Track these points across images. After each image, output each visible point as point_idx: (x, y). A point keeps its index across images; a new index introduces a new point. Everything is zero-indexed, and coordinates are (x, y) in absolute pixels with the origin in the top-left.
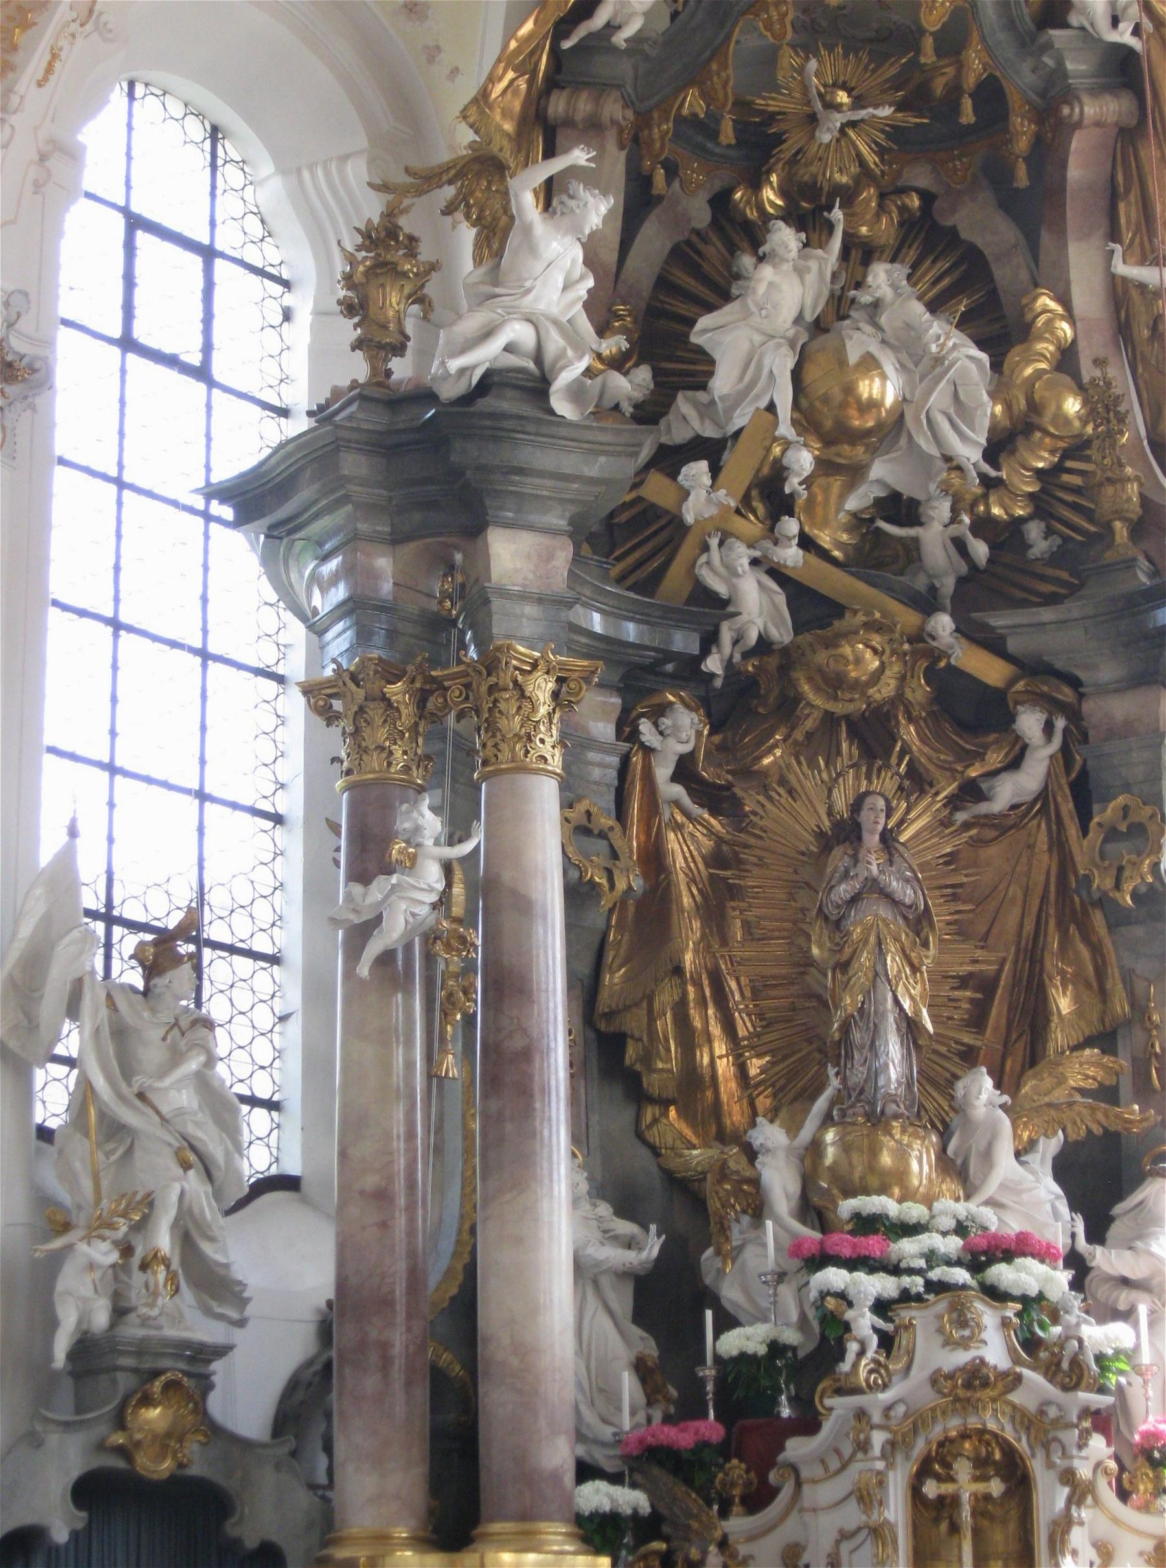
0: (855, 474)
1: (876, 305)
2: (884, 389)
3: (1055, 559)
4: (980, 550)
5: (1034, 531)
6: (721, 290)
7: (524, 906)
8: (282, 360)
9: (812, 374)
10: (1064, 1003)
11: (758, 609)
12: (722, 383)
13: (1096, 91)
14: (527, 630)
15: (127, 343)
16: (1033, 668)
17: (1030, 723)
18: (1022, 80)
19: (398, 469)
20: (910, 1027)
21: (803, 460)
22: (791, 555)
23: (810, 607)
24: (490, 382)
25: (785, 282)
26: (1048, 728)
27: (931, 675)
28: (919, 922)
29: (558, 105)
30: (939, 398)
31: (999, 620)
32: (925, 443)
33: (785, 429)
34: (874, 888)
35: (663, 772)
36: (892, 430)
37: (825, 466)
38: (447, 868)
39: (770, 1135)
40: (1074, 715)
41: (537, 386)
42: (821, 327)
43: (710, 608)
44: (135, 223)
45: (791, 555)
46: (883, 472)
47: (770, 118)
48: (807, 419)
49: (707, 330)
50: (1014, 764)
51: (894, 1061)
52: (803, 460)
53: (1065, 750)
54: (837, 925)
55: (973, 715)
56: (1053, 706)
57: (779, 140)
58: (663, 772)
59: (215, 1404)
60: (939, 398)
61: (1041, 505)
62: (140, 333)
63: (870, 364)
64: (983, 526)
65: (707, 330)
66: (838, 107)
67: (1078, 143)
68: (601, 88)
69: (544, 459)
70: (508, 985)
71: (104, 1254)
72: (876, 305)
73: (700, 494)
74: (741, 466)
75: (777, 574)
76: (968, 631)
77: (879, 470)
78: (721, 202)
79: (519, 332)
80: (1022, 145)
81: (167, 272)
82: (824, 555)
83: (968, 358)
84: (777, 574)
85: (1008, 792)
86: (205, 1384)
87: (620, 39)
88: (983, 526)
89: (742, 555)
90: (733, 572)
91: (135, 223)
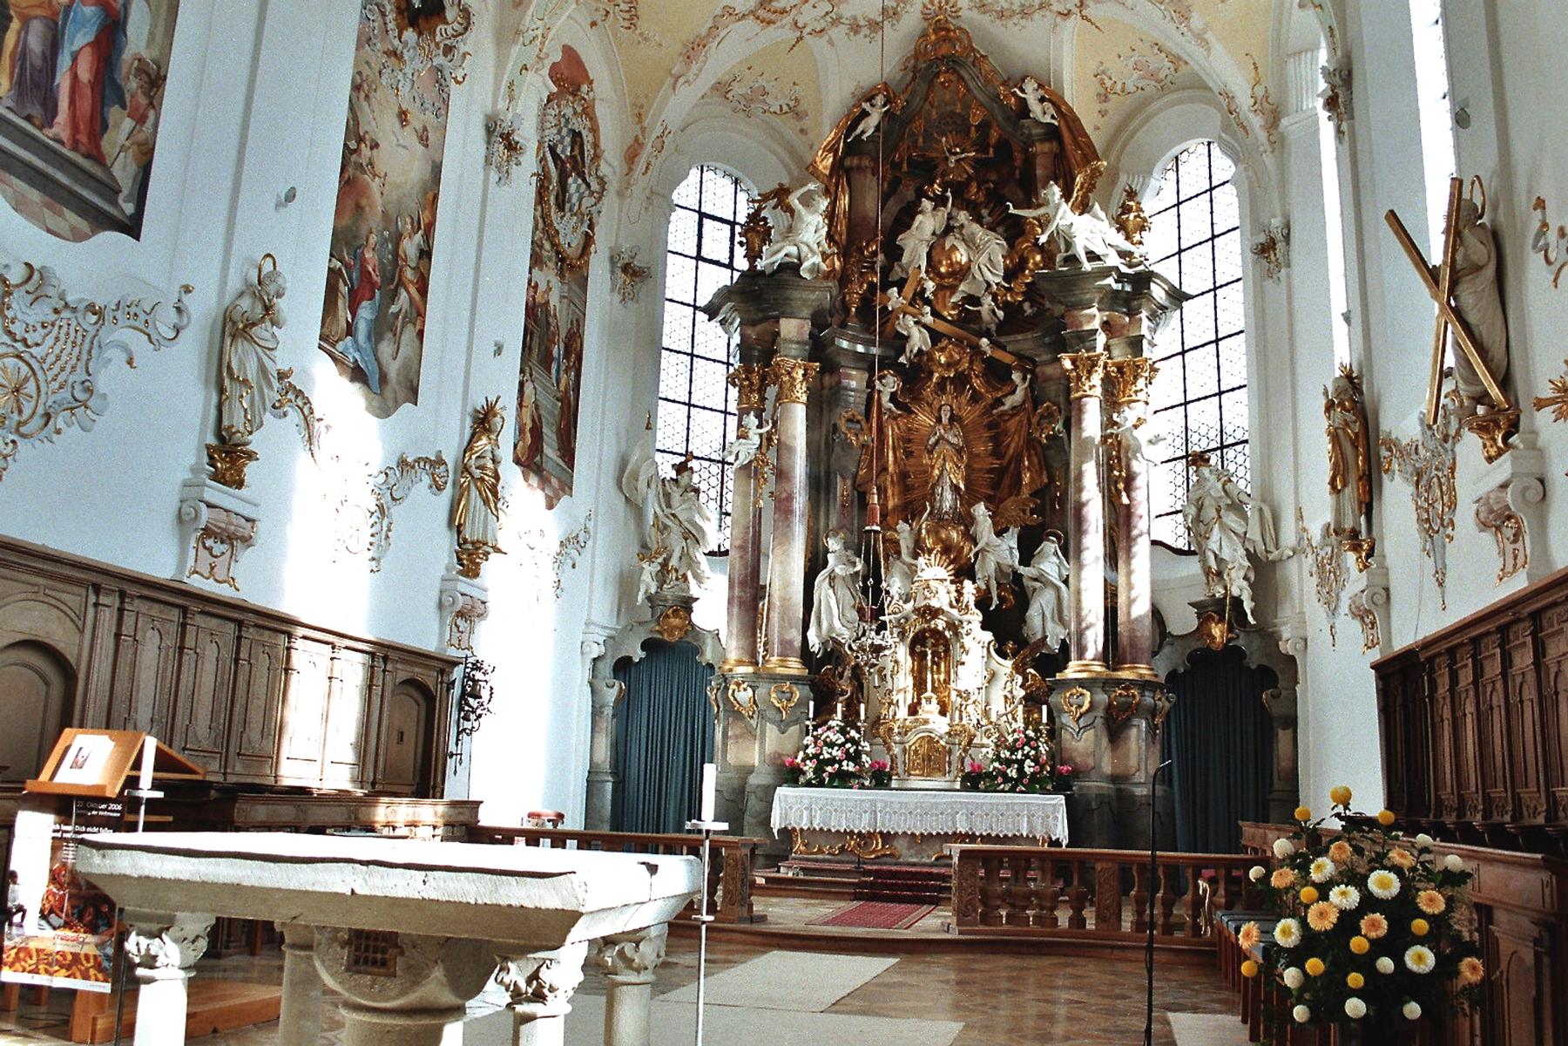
0: (953, 289)
1: (962, 226)
2: (961, 256)
3: (1035, 316)
4: (1001, 314)
5: (1026, 306)
7: (791, 450)
9: (934, 253)
10: (1027, 478)
11: (918, 340)
12: (905, 260)
13: (1042, 141)
14: (793, 353)
15: (699, 257)
16: (1019, 356)
17: (1016, 376)
19: (755, 298)
20: (955, 488)
21: (930, 286)
22: (929, 319)
23: (936, 337)
24: (783, 267)
25: (927, 222)
26: (1024, 379)
27: (984, 361)
28: (959, 451)
29: (847, 162)
30: (983, 259)
31: (1003, 340)
32: (978, 276)
33: (923, 275)
34: (941, 438)
35: (885, 399)
37: (940, 287)
38: (761, 435)
39: (902, 526)
40: (1032, 372)
43: (899, 341)
44: (702, 216)
45: (929, 319)
47: (933, 159)
49: (902, 239)
50: (1013, 392)
51: (948, 500)
52: (930, 286)
53: (1030, 385)
54: (930, 452)
55: (997, 374)
56: (1025, 372)
57: (936, 167)
58: (885, 399)
59: (695, 618)
60: (983, 259)
62: (704, 254)
63: (954, 248)
66: (956, 154)
67: (1039, 161)
68: (861, 154)
69: (796, 294)
70: (782, 474)
71: (655, 567)
72: (962, 226)
73: (894, 298)
74: (909, 290)
75: (925, 326)
76: (995, 344)
77: (961, 287)
80: (1018, 163)
82: (944, 319)
84: (925, 326)
85: (1010, 402)
86: (689, 610)
87: (864, 137)
88: (1006, 306)
89: (910, 321)
90: (907, 328)
91: (702, 216)
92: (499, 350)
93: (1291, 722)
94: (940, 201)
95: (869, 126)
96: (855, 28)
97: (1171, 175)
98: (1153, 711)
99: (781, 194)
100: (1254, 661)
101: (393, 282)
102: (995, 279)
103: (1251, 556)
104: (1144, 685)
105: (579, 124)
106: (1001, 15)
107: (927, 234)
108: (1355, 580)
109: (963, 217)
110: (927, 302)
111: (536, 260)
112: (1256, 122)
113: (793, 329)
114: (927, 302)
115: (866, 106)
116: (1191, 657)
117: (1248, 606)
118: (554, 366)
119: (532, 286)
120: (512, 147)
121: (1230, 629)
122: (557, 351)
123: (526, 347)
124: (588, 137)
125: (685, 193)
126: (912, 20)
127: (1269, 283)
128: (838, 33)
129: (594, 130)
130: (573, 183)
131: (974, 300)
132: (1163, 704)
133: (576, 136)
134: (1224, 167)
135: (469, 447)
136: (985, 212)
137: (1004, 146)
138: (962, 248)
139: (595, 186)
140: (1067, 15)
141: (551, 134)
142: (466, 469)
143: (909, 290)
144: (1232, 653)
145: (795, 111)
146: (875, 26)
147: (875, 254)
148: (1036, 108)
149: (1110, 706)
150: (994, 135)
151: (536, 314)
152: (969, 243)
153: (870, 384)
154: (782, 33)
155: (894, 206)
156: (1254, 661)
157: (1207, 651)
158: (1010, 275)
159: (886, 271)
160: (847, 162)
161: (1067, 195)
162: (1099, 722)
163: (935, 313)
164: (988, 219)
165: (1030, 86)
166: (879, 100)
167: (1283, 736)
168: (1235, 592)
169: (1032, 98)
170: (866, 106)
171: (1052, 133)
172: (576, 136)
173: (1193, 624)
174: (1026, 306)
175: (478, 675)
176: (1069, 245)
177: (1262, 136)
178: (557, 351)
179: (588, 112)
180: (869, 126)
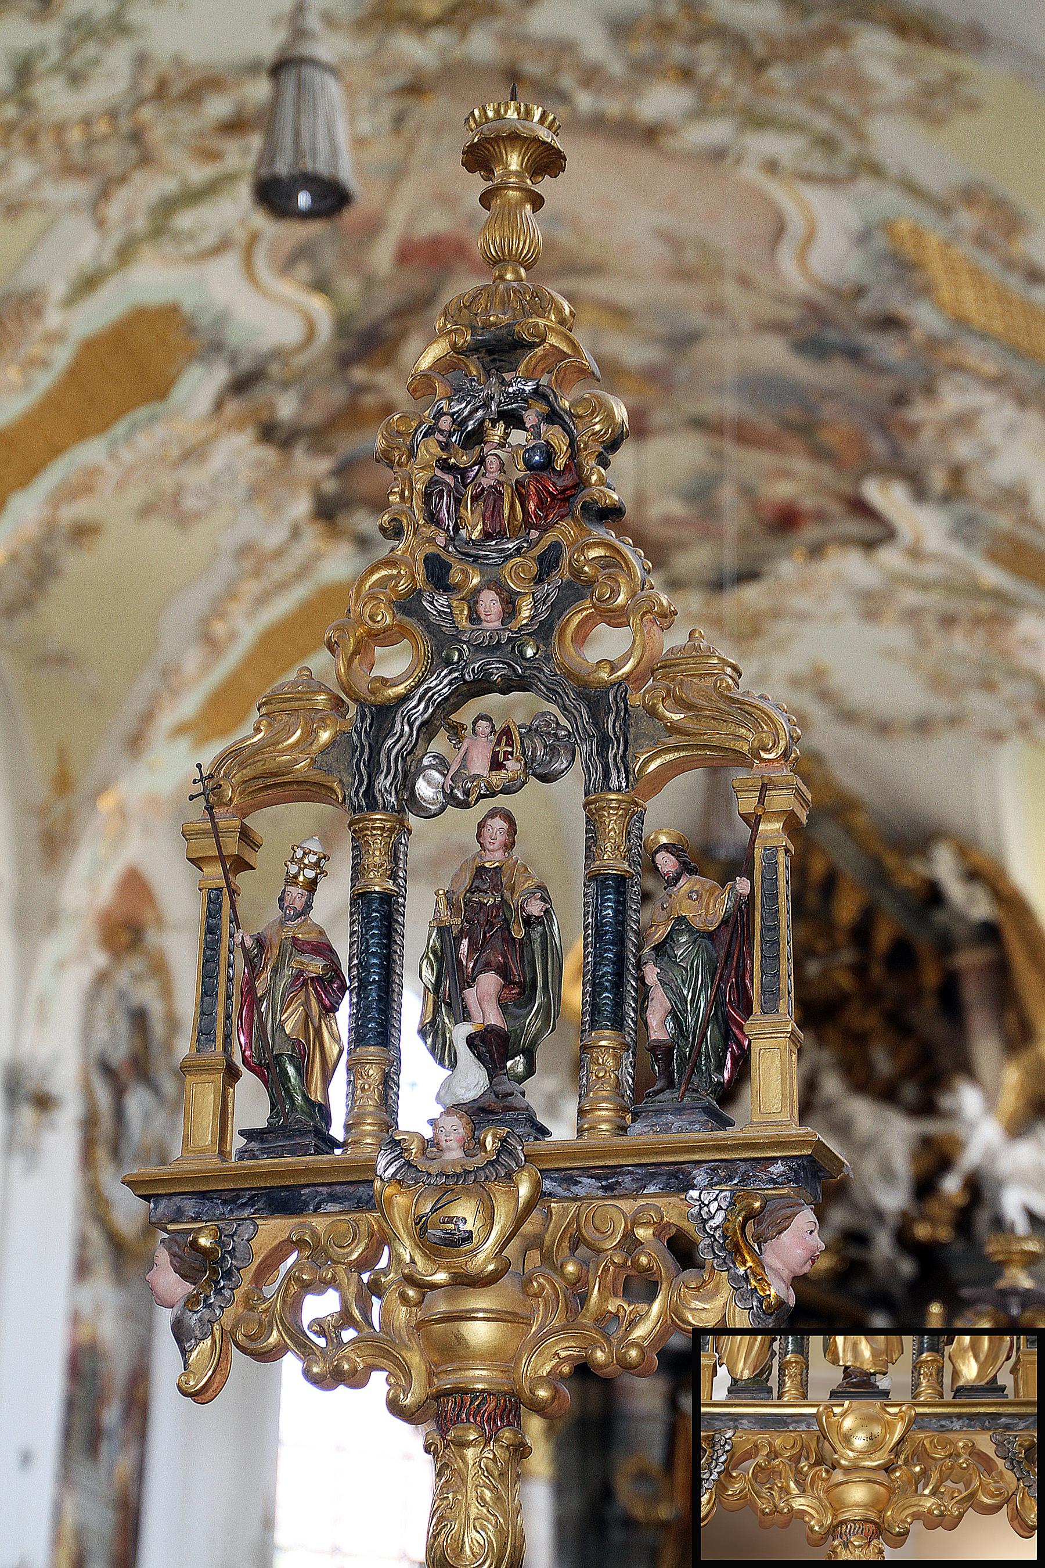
18: (923, 943)
92: (26, 1458)
105: (147, 995)
106: (883, 728)
111: (82, 1269)
118: (105, 1448)
119: (76, 1318)
120: (44, 1102)
122: (111, 1416)
123: (68, 1433)
124: (156, 1008)
129: (166, 991)
130: (137, 1101)
133: (139, 1018)
137: (902, 956)
140: (997, 737)
141: (101, 1034)
148: (956, 890)
150: (883, 937)
151: (83, 1367)
153: (673, 1404)
158: (925, 1187)
171: (989, 933)
172: (139, 1018)
178: (111, 1416)
179: (159, 969)
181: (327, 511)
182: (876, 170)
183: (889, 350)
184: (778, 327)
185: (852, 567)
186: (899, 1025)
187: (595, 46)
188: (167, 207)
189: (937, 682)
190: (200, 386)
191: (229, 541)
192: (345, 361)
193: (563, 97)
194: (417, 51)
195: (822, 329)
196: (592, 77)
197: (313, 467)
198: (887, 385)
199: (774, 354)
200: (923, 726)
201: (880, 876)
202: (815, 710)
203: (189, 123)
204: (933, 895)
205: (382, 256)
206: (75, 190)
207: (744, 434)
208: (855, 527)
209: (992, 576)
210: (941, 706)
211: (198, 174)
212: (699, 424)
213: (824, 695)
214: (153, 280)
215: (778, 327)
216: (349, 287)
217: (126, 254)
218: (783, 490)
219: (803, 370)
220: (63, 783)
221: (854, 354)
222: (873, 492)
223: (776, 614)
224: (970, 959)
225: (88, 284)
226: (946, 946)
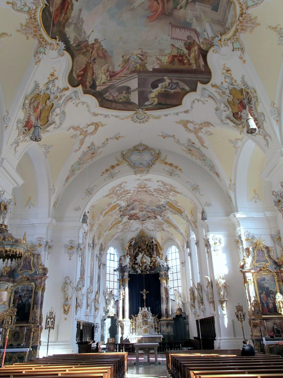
1: (145, 257)
2: (145, 261)
4: (150, 268)
5: (153, 267)
6: (137, 256)
8: (116, 265)
19: (121, 269)
21: (141, 265)
22: (141, 269)
25: (140, 256)
29: (130, 247)
36: (145, 263)
41: (127, 266)
42: (142, 258)
43: (137, 272)
45: (141, 269)
46: (145, 265)
48: (141, 262)
49: (137, 258)
52: (141, 265)
60: (148, 261)
61: (153, 265)
62: (111, 259)
64: (150, 267)
65: (137, 258)
69: (127, 270)
72: (145, 257)
78: (138, 250)
79: (126, 264)
81: (112, 259)
83: (149, 259)
88: (150, 267)
89: (138, 269)
93: (188, 324)
94: (142, 253)
95: (133, 243)
96: (132, 231)
97: (170, 249)
98: (172, 323)
99: (124, 256)
100: (183, 316)
101: (92, 280)
102: (149, 263)
103: (182, 303)
104: (171, 320)
106: (150, 230)
107: (140, 258)
108: (193, 310)
109: (145, 255)
110: (141, 267)
112: (181, 248)
113: (126, 274)
114: (141, 267)
115: (133, 241)
116: (176, 316)
117: (182, 309)
121: (180, 312)
125: (108, 252)
126: (139, 231)
127: (183, 268)
128: (130, 232)
131: (146, 266)
132: (173, 322)
134: (177, 250)
135: (96, 296)
136: (147, 253)
137: (150, 246)
138: (145, 259)
139: (101, 255)
142: (95, 299)
143: (138, 265)
144: (181, 315)
145: (123, 240)
146: (134, 231)
147: (133, 259)
148: (154, 242)
149: (167, 323)
150: (149, 245)
151: (98, 275)
152: (146, 259)
154: (123, 232)
155: (135, 252)
156: (183, 316)
157: (177, 315)
159: (135, 262)
160: (130, 247)
161: (159, 257)
162: (166, 325)
163: (141, 268)
164: (147, 254)
165: (153, 239)
166: (134, 240)
167: (187, 326)
168: (181, 307)
169: (154, 241)
170: (133, 241)
173: (176, 311)
174: (153, 267)
175: (97, 325)
176: (160, 264)
177: (182, 249)
180: (133, 243)
181: (121, 216)
182: (168, 199)
183: (164, 208)
184: (156, 206)
185: (153, 220)
186: (148, 251)
187: (152, 190)
188: (122, 197)
189: (155, 228)
190: (118, 208)
191: (115, 218)
192: (127, 207)
193: (148, 192)
194: (140, 189)
195: (158, 207)
196: (151, 192)
197: (122, 213)
198: (162, 210)
199: (155, 208)
200: (153, 230)
201: (149, 241)
202: (145, 229)
203: (125, 193)
204: (153, 242)
205: (132, 201)
206: (117, 197)
207: (149, 212)
208: (154, 218)
209: (163, 222)
210: (154, 229)
211: (124, 196)
212: (146, 211)
213: (146, 228)
214: (118, 202)
215: (156, 206)
216: (129, 202)
217: (117, 201)
218: (150, 215)
219: (156, 209)
220: (100, 234)
221: (160, 208)
222: (157, 216)
223: (146, 223)
224: (155, 247)
225: (115, 202)
226: (153, 246)
